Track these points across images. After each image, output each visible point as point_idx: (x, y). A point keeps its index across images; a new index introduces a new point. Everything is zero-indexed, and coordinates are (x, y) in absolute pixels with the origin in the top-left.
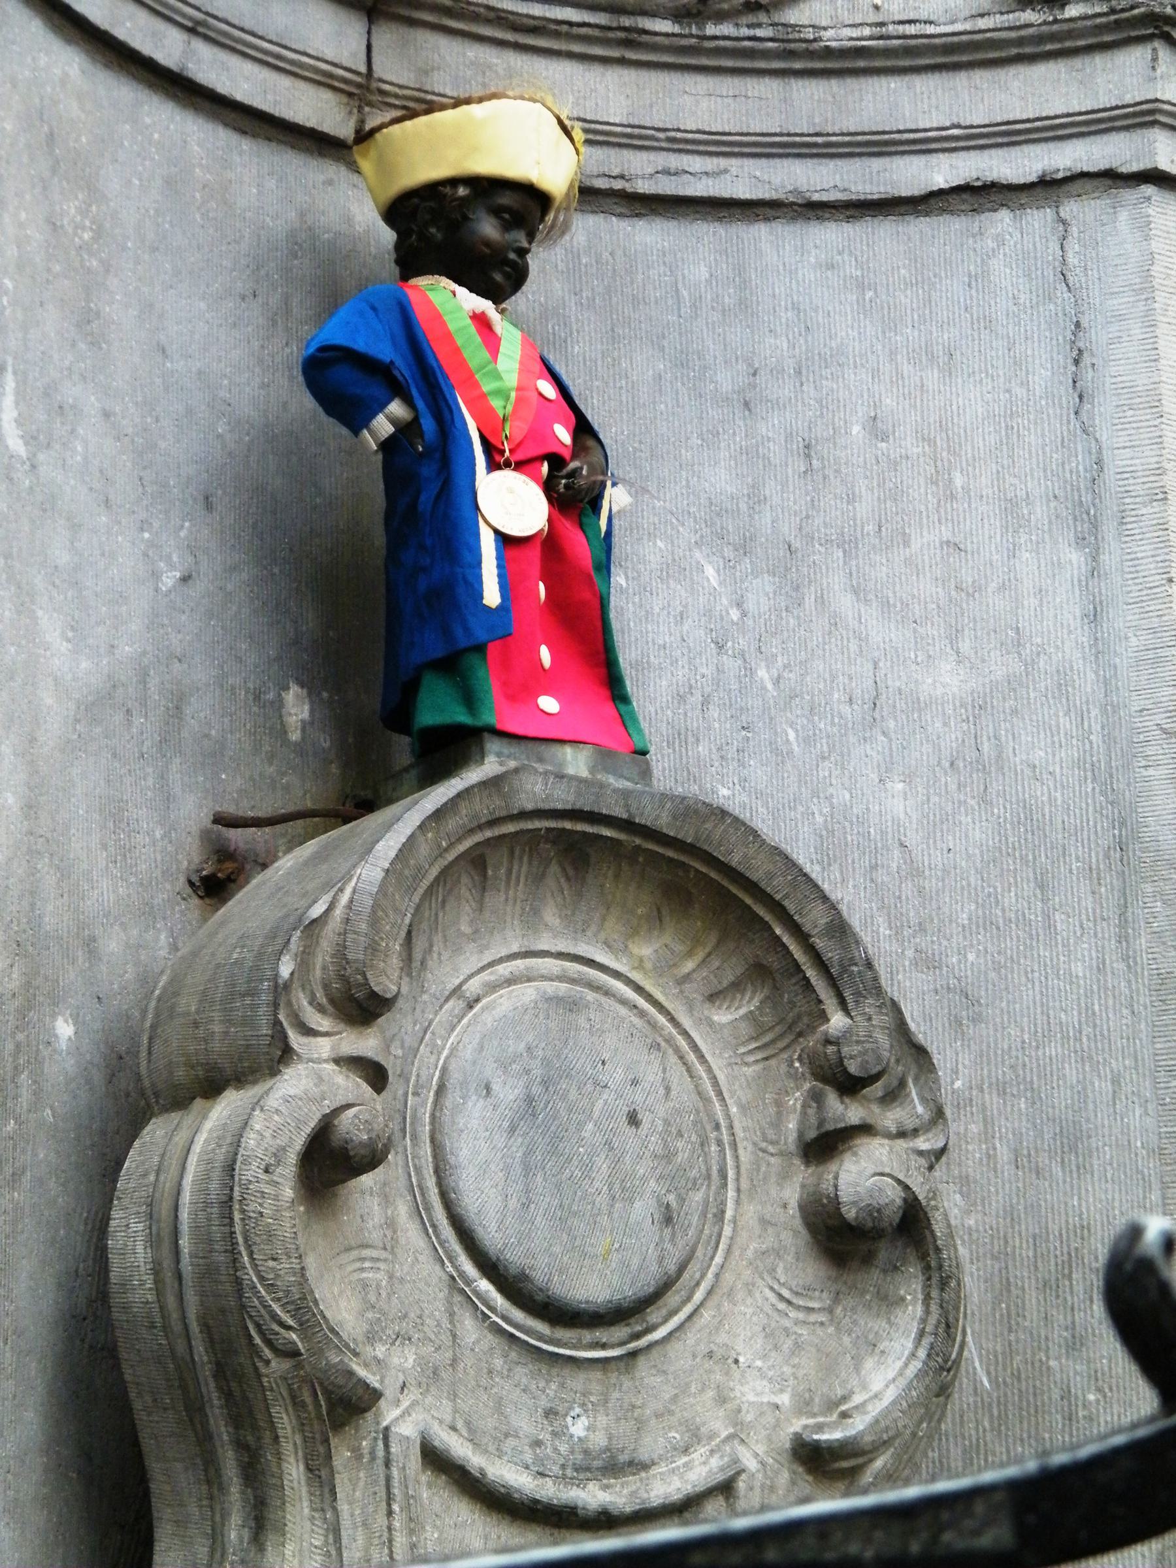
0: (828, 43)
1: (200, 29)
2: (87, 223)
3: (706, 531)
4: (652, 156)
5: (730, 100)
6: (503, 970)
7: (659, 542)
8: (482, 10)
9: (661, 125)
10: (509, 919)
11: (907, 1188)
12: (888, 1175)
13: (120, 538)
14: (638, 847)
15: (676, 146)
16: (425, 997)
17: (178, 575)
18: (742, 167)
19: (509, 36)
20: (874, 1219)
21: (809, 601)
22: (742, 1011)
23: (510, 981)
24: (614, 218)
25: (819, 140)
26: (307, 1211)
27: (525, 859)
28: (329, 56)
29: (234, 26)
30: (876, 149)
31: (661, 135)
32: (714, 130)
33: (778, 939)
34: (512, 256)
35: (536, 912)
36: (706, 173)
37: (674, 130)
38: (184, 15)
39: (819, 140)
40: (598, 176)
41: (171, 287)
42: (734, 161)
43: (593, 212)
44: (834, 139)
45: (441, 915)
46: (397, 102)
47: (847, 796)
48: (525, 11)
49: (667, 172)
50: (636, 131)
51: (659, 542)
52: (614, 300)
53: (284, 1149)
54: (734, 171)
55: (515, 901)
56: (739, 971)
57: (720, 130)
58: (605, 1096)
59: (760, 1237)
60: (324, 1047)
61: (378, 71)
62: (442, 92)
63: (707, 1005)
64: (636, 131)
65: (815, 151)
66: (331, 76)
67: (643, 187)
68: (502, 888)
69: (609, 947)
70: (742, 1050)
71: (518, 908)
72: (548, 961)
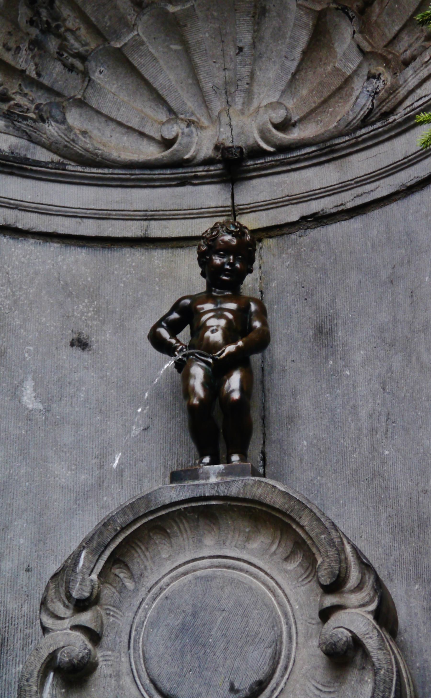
0: (398, 121)
1: (149, 218)
2: (91, 309)
3: (378, 341)
4: (352, 191)
5: (374, 158)
6: (181, 570)
7: (361, 352)
8: (273, 163)
9: (351, 178)
10: (187, 547)
11: (351, 632)
12: (342, 627)
13: (108, 423)
14: (230, 505)
15: (359, 184)
16: (144, 589)
17: (142, 428)
18: (384, 182)
19: (289, 168)
20: (333, 649)
21: (414, 359)
22: (298, 563)
23: (185, 574)
24: (343, 222)
25: (406, 160)
26: (67, 691)
27: (184, 521)
28: (213, 205)
29: (166, 211)
30: (424, 156)
31: (353, 182)
32: (370, 172)
33: (294, 530)
34: (228, 267)
35: (200, 541)
36: (372, 191)
37: (356, 178)
38: (140, 216)
39: (406, 160)
40: (333, 208)
41: (141, 318)
42: (382, 181)
43: (336, 222)
44: (410, 158)
45: (147, 554)
46: (248, 211)
47: (428, 442)
48: (290, 156)
49: (358, 196)
50: (343, 184)
51: (361, 352)
52: (343, 256)
53: (33, 671)
54: (382, 185)
55: (188, 539)
56: (292, 546)
57: (372, 171)
58: (223, 615)
59: (308, 662)
60: (67, 623)
61: (236, 202)
62: (265, 200)
63: (285, 563)
64: (343, 184)
65: (406, 165)
66: (216, 212)
67: (350, 205)
68: (179, 534)
69: (237, 548)
70: (300, 579)
71: (191, 542)
72: (205, 560)
